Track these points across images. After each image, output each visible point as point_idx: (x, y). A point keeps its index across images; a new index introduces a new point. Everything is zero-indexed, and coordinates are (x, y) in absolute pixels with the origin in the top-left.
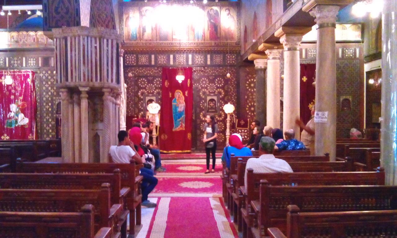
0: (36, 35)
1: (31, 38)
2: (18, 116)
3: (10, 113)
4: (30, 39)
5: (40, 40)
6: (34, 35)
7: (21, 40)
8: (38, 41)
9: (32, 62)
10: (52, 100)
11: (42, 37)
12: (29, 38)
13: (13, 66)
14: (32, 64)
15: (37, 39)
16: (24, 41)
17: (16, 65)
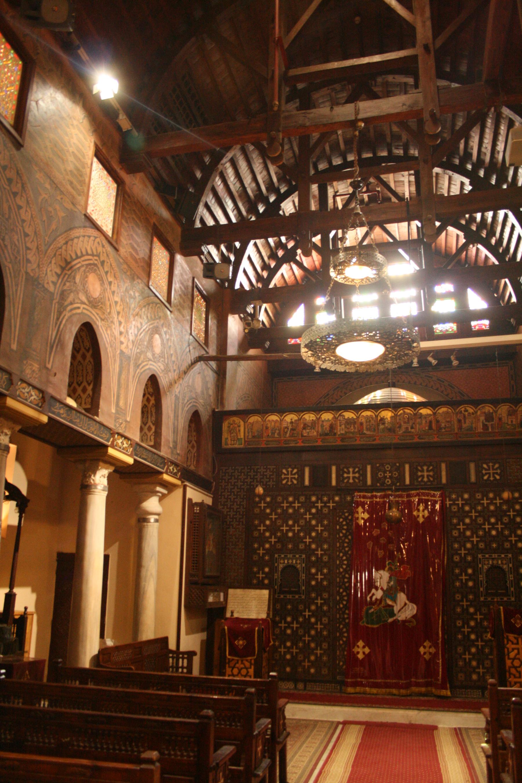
0: (434, 414)
1: (424, 422)
2: (394, 600)
3: (373, 591)
4: (420, 424)
5: (443, 425)
6: (430, 415)
7: (400, 427)
8: (439, 428)
9: (425, 474)
10: (475, 558)
11: (448, 420)
12: (418, 420)
13: (383, 484)
14: (425, 479)
15: (438, 422)
16: (407, 428)
17: (388, 481)
